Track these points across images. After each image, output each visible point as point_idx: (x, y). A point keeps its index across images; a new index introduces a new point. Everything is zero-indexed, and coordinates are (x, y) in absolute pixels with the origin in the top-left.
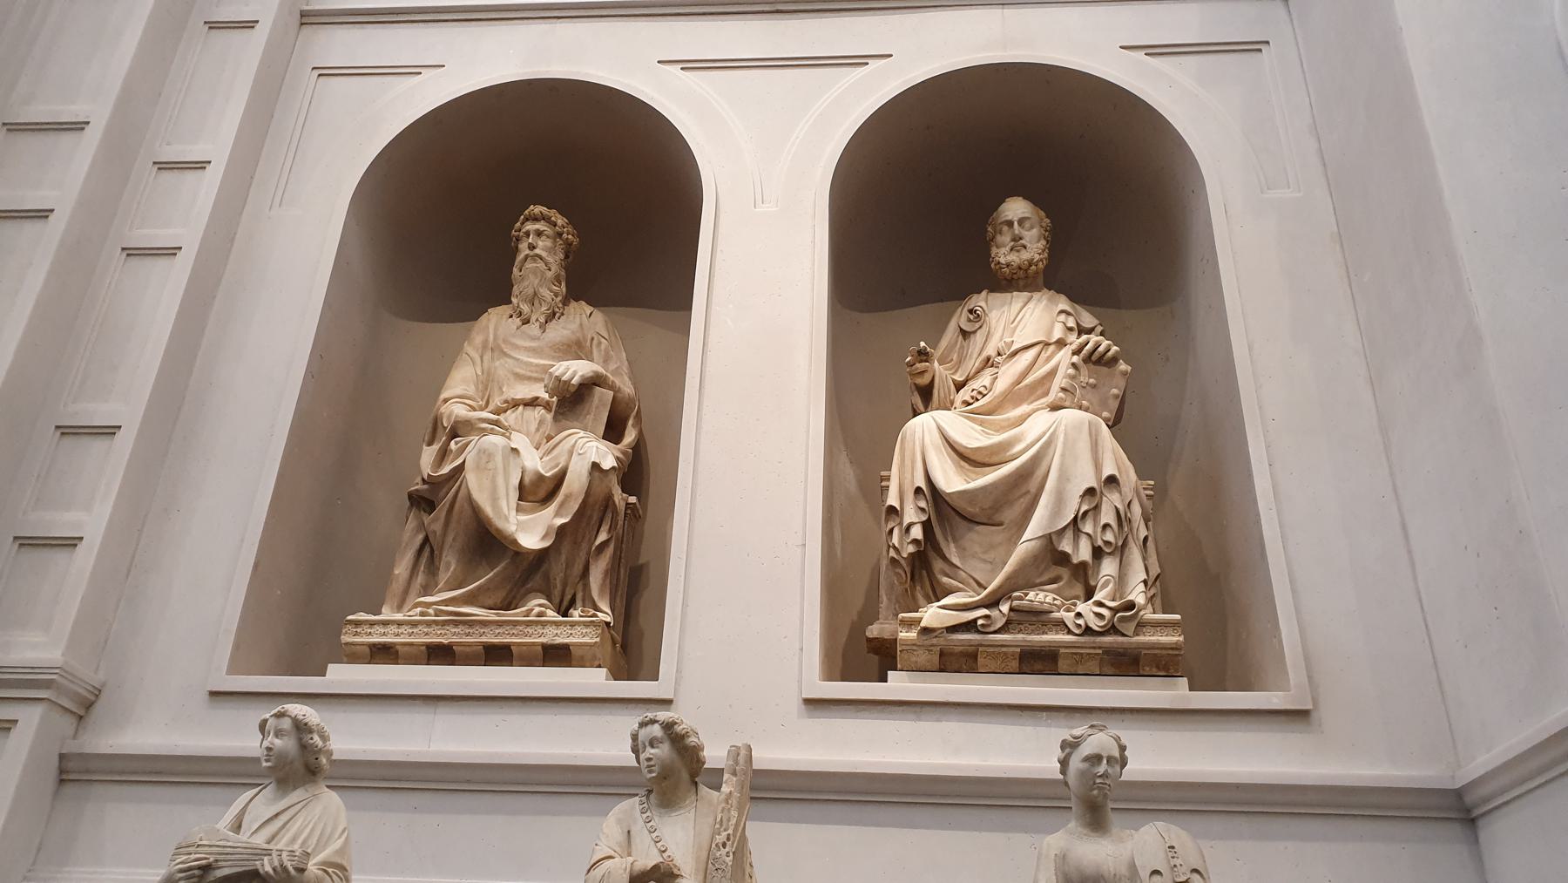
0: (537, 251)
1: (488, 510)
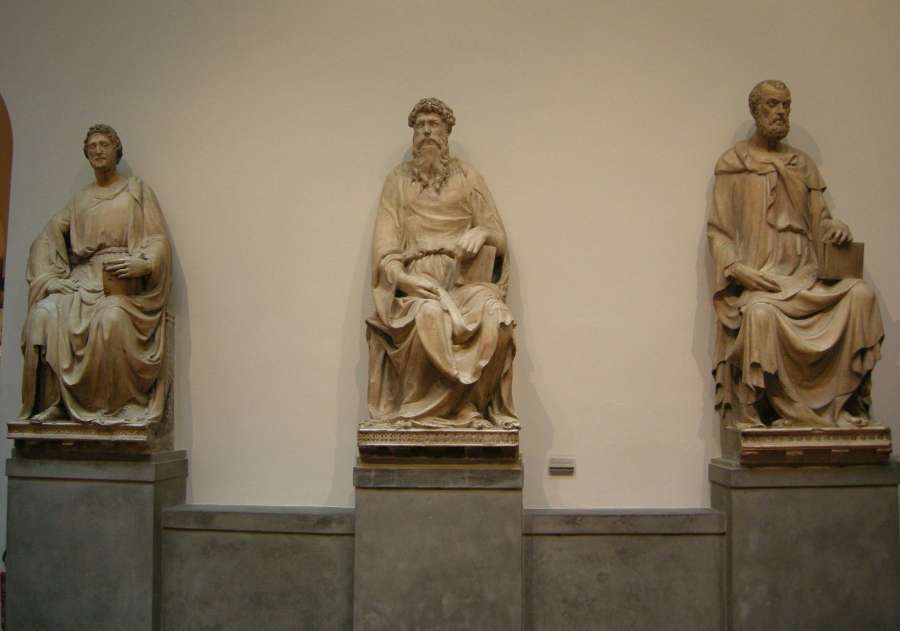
0: (432, 137)
1: (437, 358)
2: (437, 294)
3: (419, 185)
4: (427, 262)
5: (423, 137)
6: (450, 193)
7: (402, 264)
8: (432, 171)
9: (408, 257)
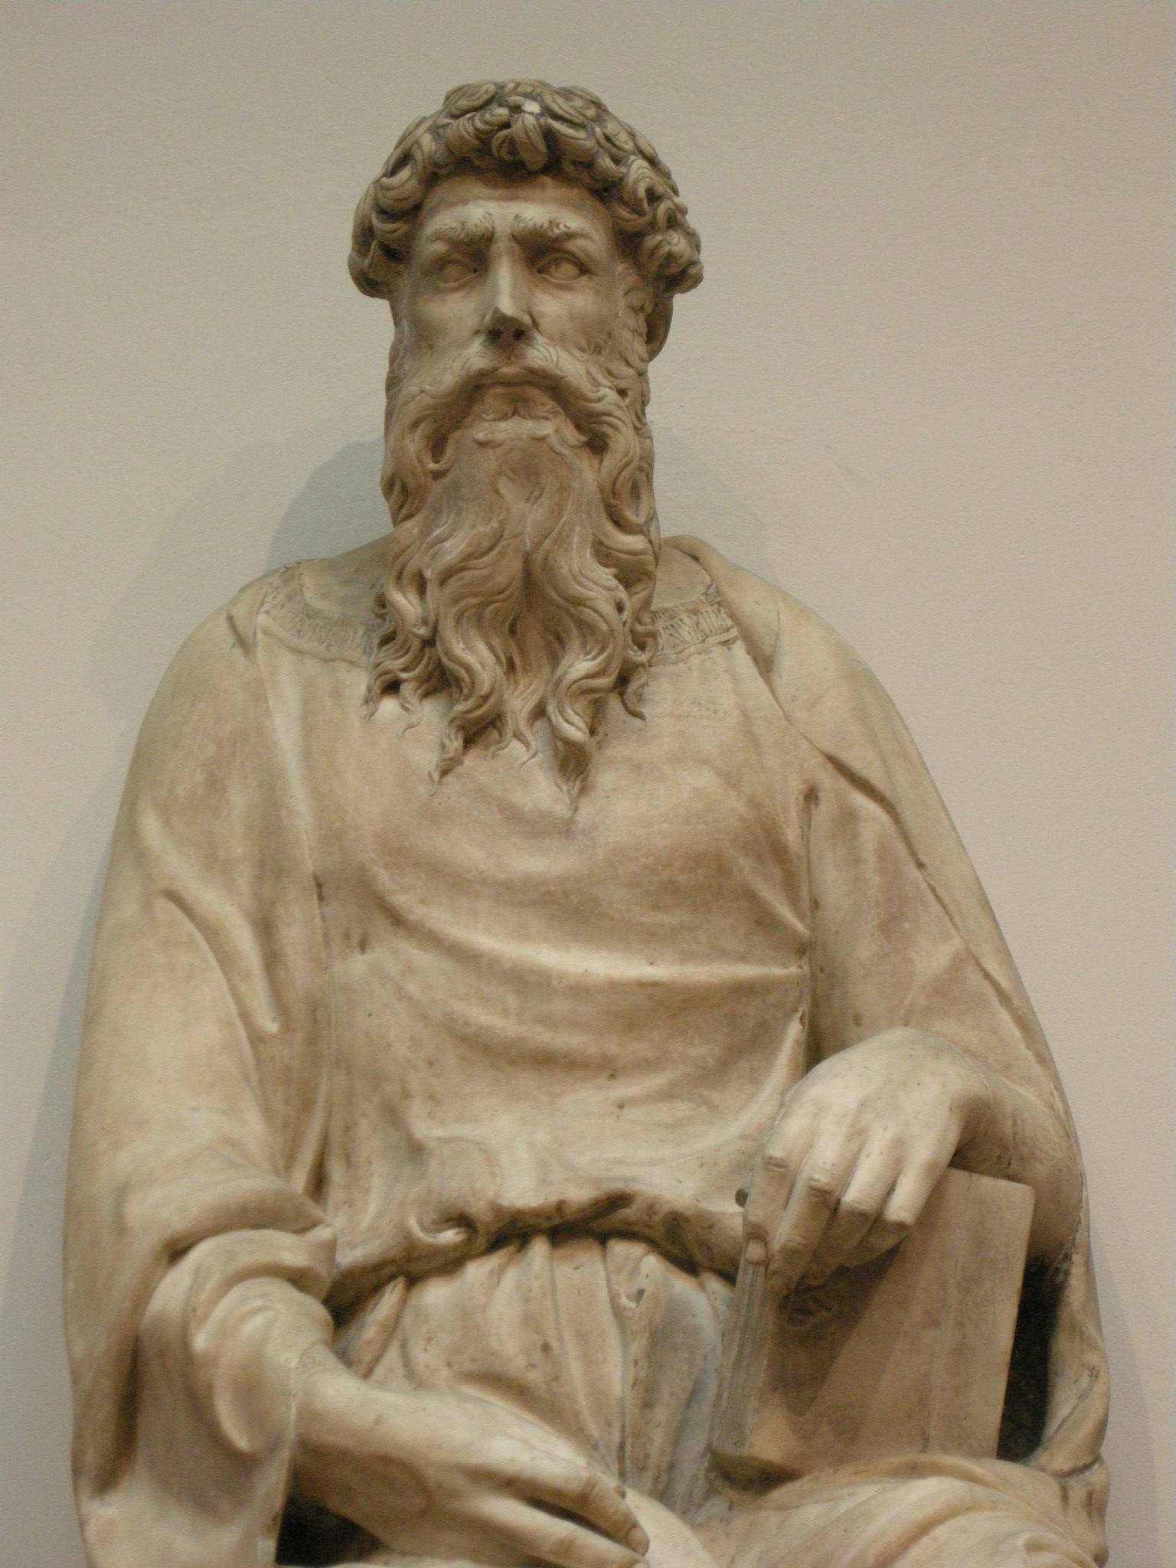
0: (541, 354)
2: (622, 1531)
3: (421, 726)
4: (497, 1294)
5: (476, 356)
6: (660, 787)
7: (322, 1313)
8: (533, 612)
9: (349, 1257)
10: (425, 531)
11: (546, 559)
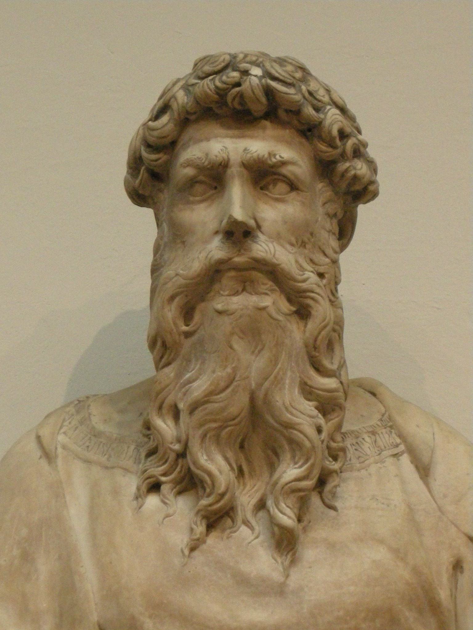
0: (263, 248)
3: (177, 514)
5: (216, 249)
8: (257, 434)
10: (179, 375)
11: (266, 395)
